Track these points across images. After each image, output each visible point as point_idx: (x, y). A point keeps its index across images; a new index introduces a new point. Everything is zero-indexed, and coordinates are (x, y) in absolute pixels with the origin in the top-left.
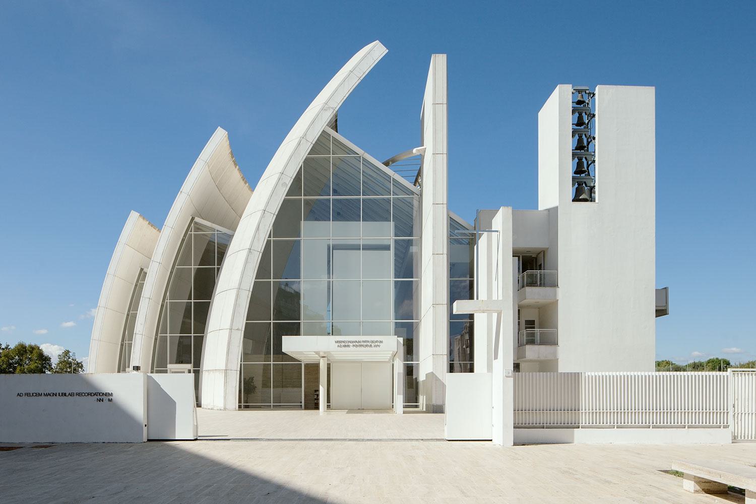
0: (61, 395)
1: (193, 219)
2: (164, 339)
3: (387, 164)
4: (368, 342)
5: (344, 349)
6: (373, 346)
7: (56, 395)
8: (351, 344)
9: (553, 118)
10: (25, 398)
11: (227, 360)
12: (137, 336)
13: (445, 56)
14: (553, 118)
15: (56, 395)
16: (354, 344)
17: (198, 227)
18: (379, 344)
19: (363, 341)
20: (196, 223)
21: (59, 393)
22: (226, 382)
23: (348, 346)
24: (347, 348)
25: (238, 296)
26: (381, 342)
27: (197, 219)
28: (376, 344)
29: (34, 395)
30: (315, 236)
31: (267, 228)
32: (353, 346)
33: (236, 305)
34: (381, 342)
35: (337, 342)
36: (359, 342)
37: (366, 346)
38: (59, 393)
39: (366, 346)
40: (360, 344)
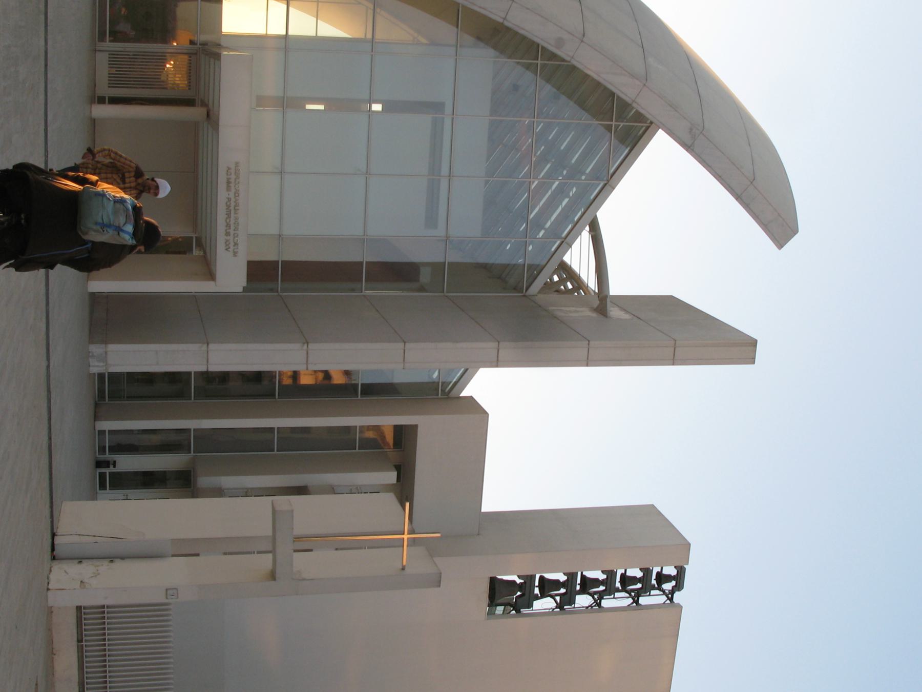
6: (228, 238)
8: (232, 195)
16: (233, 200)
18: (231, 250)
19: (237, 219)
23: (228, 188)
24: (225, 185)
26: (235, 254)
32: (229, 199)
34: (235, 254)
35: (237, 164)
37: (228, 225)
39: (228, 225)
40: (233, 212)
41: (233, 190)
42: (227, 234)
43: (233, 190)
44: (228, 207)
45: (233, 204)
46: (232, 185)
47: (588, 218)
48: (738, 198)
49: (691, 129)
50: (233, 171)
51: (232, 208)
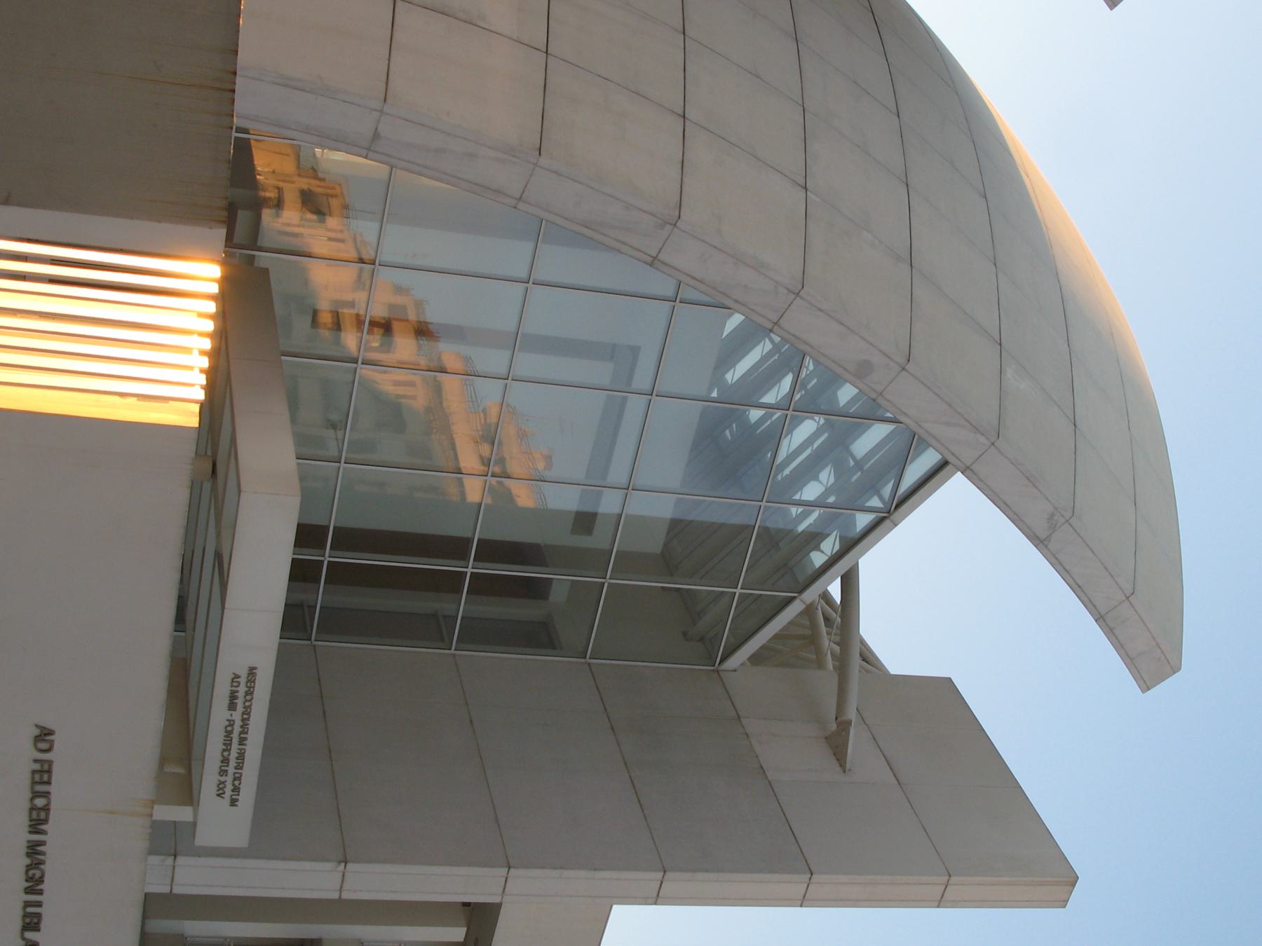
0: (30, 910)
4: (239, 767)
7: (29, 891)
8: (237, 716)
10: (25, 755)
15: (29, 891)
19: (241, 756)
21: (39, 904)
23: (232, 706)
24: (226, 702)
26: (233, 802)
28: (229, 787)
29: (40, 802)
32: (231, 723)
34: (233, 802)
35: (252, 672)
36: (242, 741)
37: (225, 761)
38: (39, 904)
39: (225, 761)
41: (240, 708)
42: (223, 772)
43: (240, 708)
44: (229, 734)
45: (237, 729)
46: (240, 703)
47: (843, 566)
48: (1100, 618)
49: (1052, 515)
50: (243, 680)
51: (235, 736)
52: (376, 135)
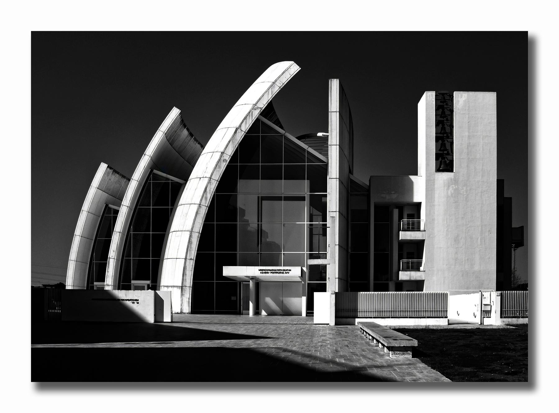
1: (152, 171)
2: (128, 262)
3: (299, 138)
5: (264, 275)
9: (426, 105)
11: (183, 279)
12: (111, 260)
13: (338, 81)
14: (426, 105)
17: (156, 177)
19: (278, 270)
20: (154, 174)
22: (182, 295)
23: (268, 273)
25: (191, 236)
27: (155, 171)
30: (248, 192)
31: (212, 190)
33: (190, 242)
39: (280, 273)
42: (283, 273)
44: (273, 273)
52: (191, 259)
